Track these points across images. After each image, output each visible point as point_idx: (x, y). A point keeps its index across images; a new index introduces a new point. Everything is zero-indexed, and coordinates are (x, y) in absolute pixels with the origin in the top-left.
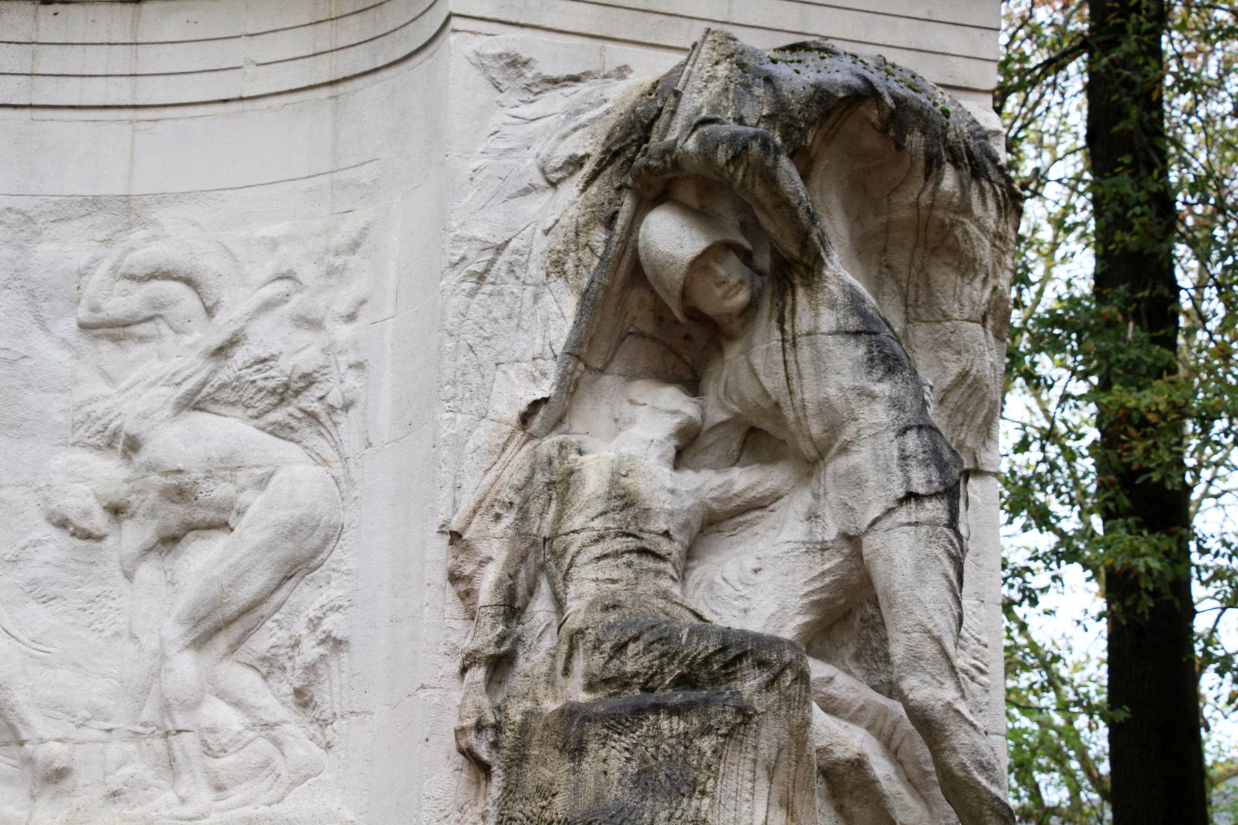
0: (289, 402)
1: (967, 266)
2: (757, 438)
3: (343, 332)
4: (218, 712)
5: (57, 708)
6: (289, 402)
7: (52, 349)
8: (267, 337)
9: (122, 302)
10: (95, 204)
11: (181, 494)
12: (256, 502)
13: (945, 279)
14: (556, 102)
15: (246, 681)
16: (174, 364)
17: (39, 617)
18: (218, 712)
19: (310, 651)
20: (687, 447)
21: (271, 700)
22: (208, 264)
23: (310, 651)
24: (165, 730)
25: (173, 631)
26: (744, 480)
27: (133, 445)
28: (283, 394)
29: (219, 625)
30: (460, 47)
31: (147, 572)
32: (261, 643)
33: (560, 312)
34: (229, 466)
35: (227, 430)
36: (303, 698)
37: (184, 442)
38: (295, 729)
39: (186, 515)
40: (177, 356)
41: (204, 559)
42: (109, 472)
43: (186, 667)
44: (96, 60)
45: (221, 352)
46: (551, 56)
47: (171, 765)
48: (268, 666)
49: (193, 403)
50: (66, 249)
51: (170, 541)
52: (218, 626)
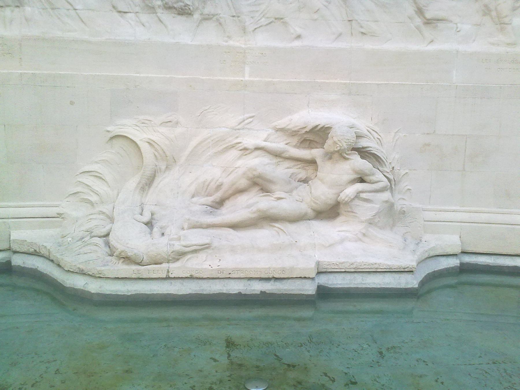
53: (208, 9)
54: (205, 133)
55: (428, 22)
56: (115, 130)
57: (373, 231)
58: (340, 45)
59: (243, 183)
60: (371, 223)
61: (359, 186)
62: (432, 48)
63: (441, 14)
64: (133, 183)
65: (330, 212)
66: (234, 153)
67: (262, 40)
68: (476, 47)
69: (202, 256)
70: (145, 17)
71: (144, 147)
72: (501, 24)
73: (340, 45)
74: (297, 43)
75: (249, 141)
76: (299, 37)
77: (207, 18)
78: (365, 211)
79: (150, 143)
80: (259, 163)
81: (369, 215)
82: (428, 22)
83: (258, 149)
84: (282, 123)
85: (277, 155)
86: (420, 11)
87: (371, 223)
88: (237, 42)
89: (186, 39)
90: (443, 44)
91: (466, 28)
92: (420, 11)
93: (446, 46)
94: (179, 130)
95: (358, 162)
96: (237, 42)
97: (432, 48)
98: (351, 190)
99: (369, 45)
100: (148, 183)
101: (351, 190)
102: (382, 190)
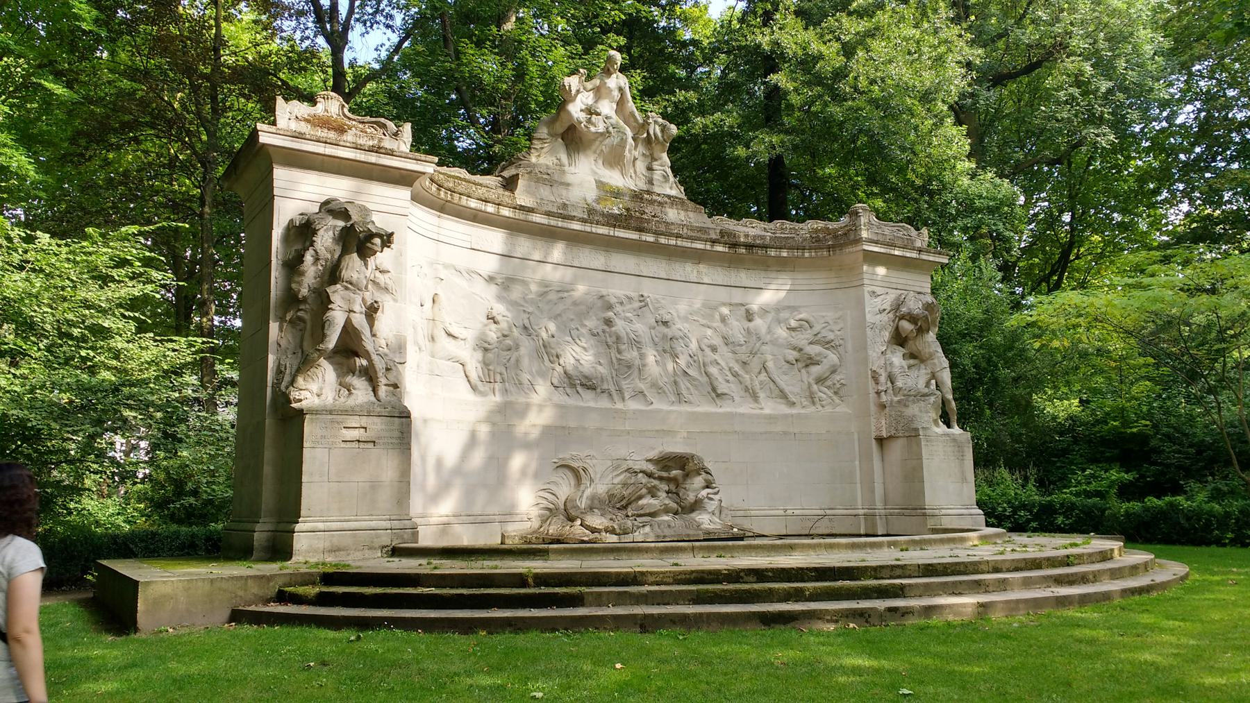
0: (827, 344)
5: (792, 393)
6: (827, 344)
10: (789, 307)
12: (825, 361)
14: (879, 299)
17: (786, 378)
19: (838, 386)
22: (811, 319)
23: (838, 386)
24: (812, 398)
25: (812, 382)
26: (912, 362)
27: (801, 350)
28: (828, 343)
29: (820, 380)
31: (803, 371)
33: (887, 335)
34: (819, 354)
35: (816, 349)
36: (836, 393)
37: (814, 350)
38: (835, 398)
39: (810, 362)
40: (808, 335)
41: (815, 370)
42: (795, 354)
43: (815, 387)
48: (829, 387)
49: (811, 343)
51: (807, 366)
53: (605, 386)
55: (718, 396)
63: (725, 391)
67: (633, 405)
68: (741, 410)
70: (569, 391)
72: (755, 397)
74: (650, 407)
82: (718, 396)
85: (650, 475)
86: (714, 390)
88: (619, 406)
89: (592, 404)
90: (726, 408)
93: (728, 410)
96: (619, 406)
97: (721, 410)
101: (704, 492)
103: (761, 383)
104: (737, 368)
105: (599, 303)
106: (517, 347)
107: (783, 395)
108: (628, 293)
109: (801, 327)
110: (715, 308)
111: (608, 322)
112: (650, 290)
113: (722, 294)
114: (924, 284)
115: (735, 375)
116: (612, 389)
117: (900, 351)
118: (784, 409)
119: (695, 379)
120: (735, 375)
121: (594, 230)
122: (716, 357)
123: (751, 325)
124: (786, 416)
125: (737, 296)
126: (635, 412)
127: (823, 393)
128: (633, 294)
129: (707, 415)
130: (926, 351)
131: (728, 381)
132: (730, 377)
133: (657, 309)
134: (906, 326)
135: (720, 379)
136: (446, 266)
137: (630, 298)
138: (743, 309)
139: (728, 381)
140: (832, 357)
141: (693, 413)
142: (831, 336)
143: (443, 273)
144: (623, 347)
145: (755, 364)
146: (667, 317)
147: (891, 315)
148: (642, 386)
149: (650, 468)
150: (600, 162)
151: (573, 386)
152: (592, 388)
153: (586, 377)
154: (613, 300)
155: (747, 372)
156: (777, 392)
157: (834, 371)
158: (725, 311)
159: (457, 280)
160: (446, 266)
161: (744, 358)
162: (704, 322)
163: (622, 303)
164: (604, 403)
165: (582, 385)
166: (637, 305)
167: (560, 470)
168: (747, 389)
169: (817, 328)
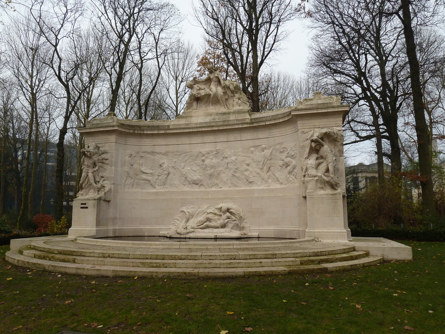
0: (292, 157)
1: (338, 142)
2: (322, 157)
3: (295, 151)
4: (291, 179)
7: (278, 154)
8: (291, 152)
9: (282, 150)
10: (279, 143)
11: (287, 164)
13: (337, 143)
15: (292, 176)
16: (284, 155)
17: (279, 173)
18: (291, 179)
20: (317, 159)
21: (294, 178)
22: (287, 147)
26: (321, 161)
28: (292, 156)
29: (290, 173)
30: (299, 131)
32: (293, 174)
33: (308, 150)
34: (289, 161)
35: (289, 159)
38: (295, 180)
40: (285, 154)
41: (289, 168)
43: (288, 176)
44: (277, 133)
45: (288, 153)
46: (306, 131)
47: (288, 182)
48: (293, 175)
49: (287, 157)
50: (278, 147)
51: (287, 167)
52: (290, 173)
54: (200, 210)
55: (250, 182)
56: (182, 210)
57: (233, 230)
58: (230, 189)
59: (205, 220)
60: (232, 228)
61: (228, 220)
62: (251, 188)
63: (252, 181)
64: (184, 221)
65: (224, 226)
66: (206, 214)
67: (213, 189)
69: (192, 233)
70: (189, 186)
71: (187, 213)
72: (266, 182)
73: (230, 189)
74: (220, 189)
75: (209, 211)
76: (221, 188)
77: (202, 185)
78: (230, 225)
79: (188, 212)
80: (210, 216)
81: (231, 226)
83: (210, 213)
84: (217, 207)
85: (215, 214)
86: (247, 180)
87: (232, 228)
89: (197, 190)
90: (254, 187)
91: (259, 183)
92: (247, 180)
94: (195, 209)
95: (228, 214)
98: (226, 221)
99: (237, 189)
100: (188, 221)
102: (235, 220)
103: (269, 176)
104: (258, 171)
105: (200, 155)
106: (169, 174)
107: (278, 180)
108: (210, 149)
109: (284, 151)
110: (249, 149)
111: (203, 161)
112: (219, 146)
113: (251, 143)
114: (339, 122)
115: (258, 174)
116: (205, 184)
117: (315, 156)
118: (278, 186)
119: (239, 177)
120: (258, 174)
121: (193, 131)
122: (249, 168)
123: (263, 153)
124: (276, 189)
125: (257, 142)
126: (213, 191)
127: (292, 178)
128: (212, 149)
129: (243, 191)
130: (324, 155)
131: (254, 177)
132: (256, 175)
133: (223, 153)
134: (313, 145)
135: (251, 176)
136: (143, 152)
137: (212, 151)
138: (260, 147)
139: (254, 177)
140: (294, 162)
141: (238, 190)
142: (293, 153)
143: (143, 155)
144: (208, 169)
145: (265, 168)
146: (226, 156)
147: (310, 141)
148: (216, 182)
149: (216, 212)
150: (211, 104)
151: (190, 184)
152: (197, 184)
153: (194, 181)
154: (204, 153)
155: (263, 172)
156: (276, 179)
157: (294, 168)
158: (252, 149)
159: (149, 156)
160: (143, 152)
161: (261, 167)
162: (244, 155)
163: (208, 153)
164: (202, 189)
165: (193, 183)
166: (215, 153)
167: (182, 213)
168: (263, 179)
169: (288, 151)
